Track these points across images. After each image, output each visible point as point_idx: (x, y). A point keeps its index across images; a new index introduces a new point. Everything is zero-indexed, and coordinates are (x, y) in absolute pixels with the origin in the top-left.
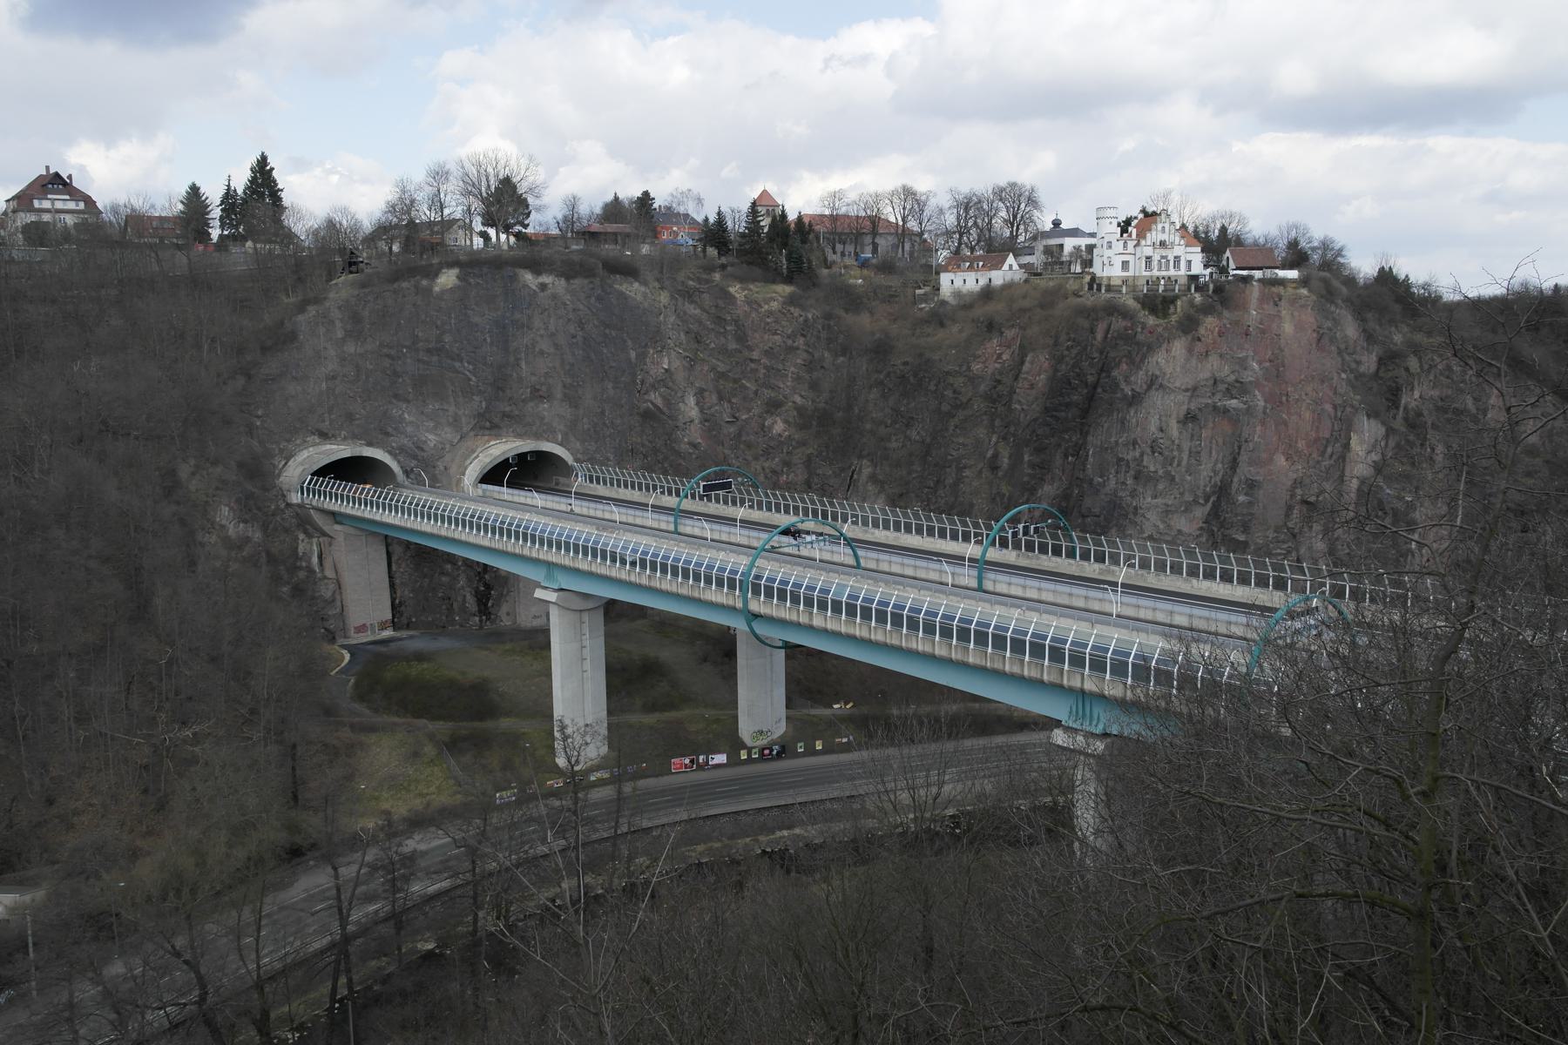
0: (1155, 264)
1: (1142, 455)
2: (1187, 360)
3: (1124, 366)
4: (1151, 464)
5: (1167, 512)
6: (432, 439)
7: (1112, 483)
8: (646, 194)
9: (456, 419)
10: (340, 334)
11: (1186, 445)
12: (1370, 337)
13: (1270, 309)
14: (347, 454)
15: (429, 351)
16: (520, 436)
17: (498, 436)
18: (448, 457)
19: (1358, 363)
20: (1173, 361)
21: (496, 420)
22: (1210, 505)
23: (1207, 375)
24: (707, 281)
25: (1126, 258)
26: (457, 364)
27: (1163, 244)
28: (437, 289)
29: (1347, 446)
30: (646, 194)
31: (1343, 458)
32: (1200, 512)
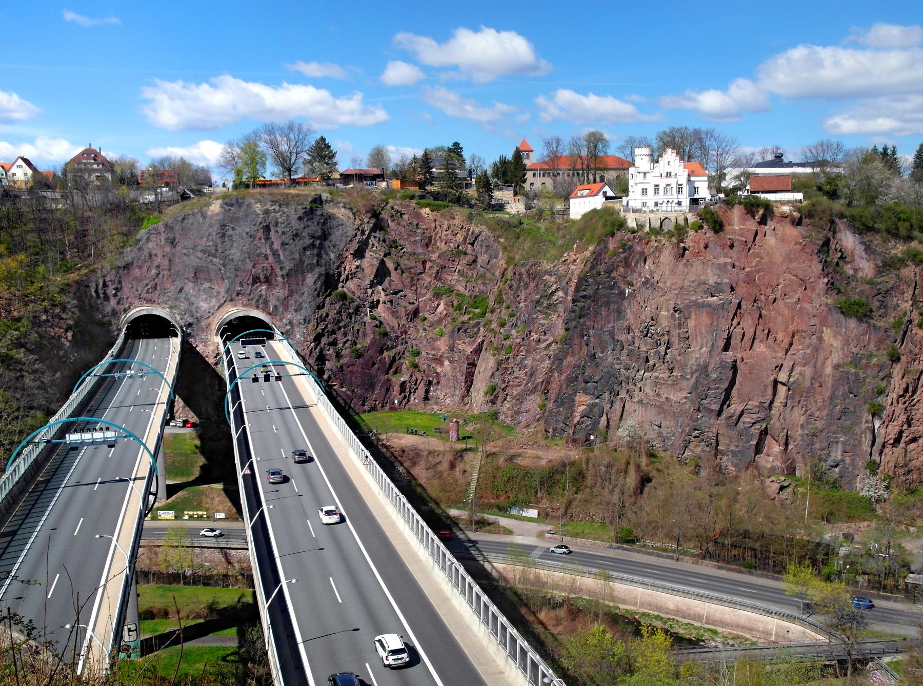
0: (661, 190)
1: (633, 338)
2: (675, 266)
3: (622, 270)
4: (644, 347)
5: (656, 382)
6: (204, 306)
7: (610, 359)
8: (456, 145)
9: (218, 293)
10: (163, 242)
11: (675, 332)
12: (868, 249)
13: (752, 225)
14: (144, 313)
15: (201, 251)
16: (245, 306)
17: (235, 306)
18: (211, 318)
19: (856, 270)
20: (662, 266)
21: (234, 296)
22: (693, 381)
23: (692, 277)
24: (407, 206)
25: (644, 186)
26: (215, 260)
27: (669, 175)
28: (209, 213)
29: (820, 339)
30: (456, 145)
31: (816, 350)
32: (687, 385)
